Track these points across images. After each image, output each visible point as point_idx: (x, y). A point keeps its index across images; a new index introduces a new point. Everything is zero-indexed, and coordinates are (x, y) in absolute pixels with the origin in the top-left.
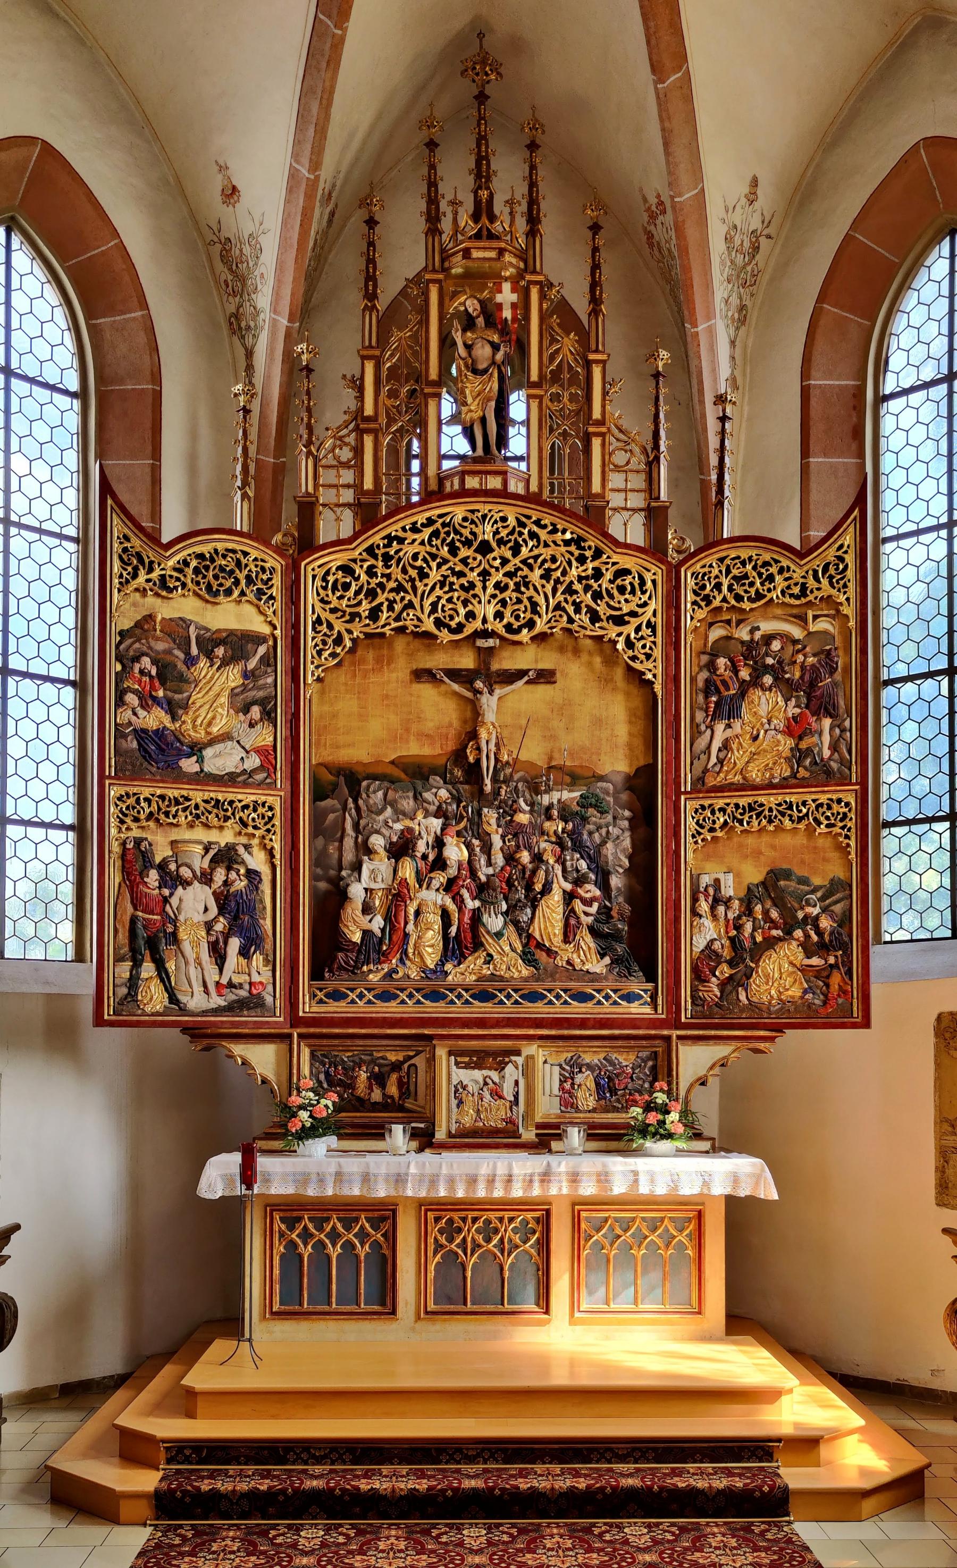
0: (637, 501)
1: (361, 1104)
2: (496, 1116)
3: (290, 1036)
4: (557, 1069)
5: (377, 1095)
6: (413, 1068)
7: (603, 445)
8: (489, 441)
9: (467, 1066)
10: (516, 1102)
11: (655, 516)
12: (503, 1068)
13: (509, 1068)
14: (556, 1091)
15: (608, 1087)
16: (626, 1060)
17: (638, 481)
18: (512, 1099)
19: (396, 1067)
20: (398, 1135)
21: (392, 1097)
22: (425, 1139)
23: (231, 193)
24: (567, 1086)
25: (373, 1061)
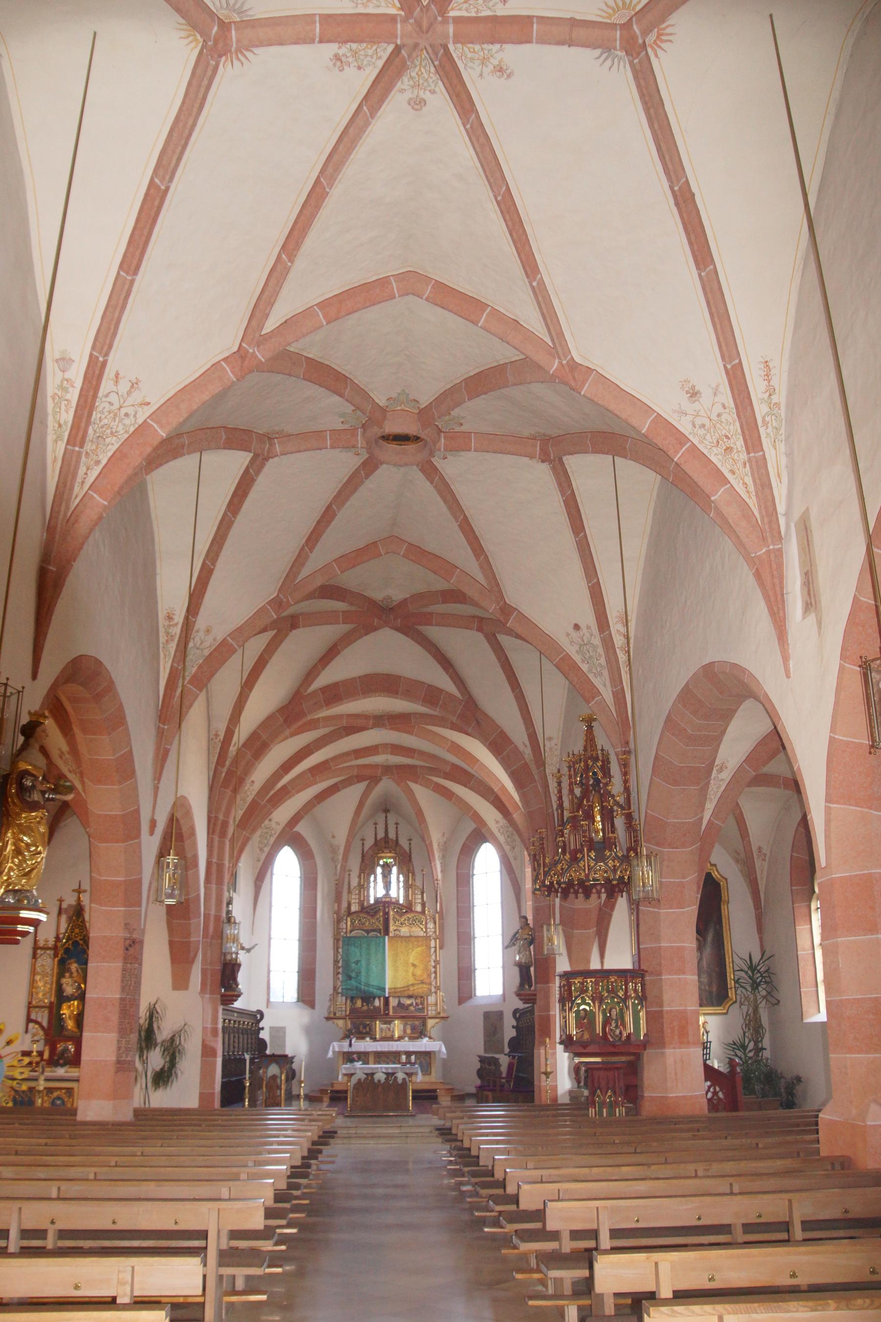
0: (420, 901)
1: (361, 1033)
2: (389, 1034)
8: (387, 885)
11: (423, 905)
15: (413, 1028)
16: (417, 1023)
17: (420, 897)
20: (368, 1039)
22: (374, 1039)
23: (333, 837)
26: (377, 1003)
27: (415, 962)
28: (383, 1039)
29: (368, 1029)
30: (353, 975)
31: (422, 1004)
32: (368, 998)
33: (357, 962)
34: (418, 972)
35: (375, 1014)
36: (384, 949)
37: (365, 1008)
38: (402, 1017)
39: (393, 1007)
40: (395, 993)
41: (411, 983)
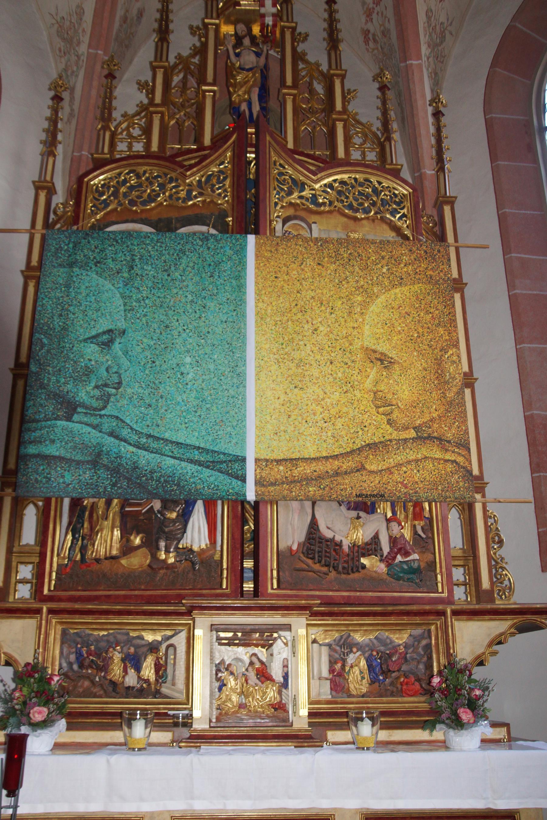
3: (38, 611)
4: (325, 650)
5: (131, 680)
6: (171, 651)
7: (345, 127)
9: (230, 643)
10: (285, 685)
12: (271, 645)
13: (278, 645)
14: (325, 673)
15: (381, 666)
16: (400, 638)
18: (282, 680)
19: (153, 648)
21: (147, 681)
24: (338, 666)
25: (130, 641)
26: (197, 534)
27: (383, 347)
28: (228, 733)
29: (148, 671)
30: (85, 393)
31: (424, 542)
32: (152, 516)
33: (107, 340)
34: (404, 389)
35: (183, 591)
36: (241, 288)
37: (138, 561)
38: (324, 611)
39: (282, 557)
40: (293, 478)
41: (369, 437)
